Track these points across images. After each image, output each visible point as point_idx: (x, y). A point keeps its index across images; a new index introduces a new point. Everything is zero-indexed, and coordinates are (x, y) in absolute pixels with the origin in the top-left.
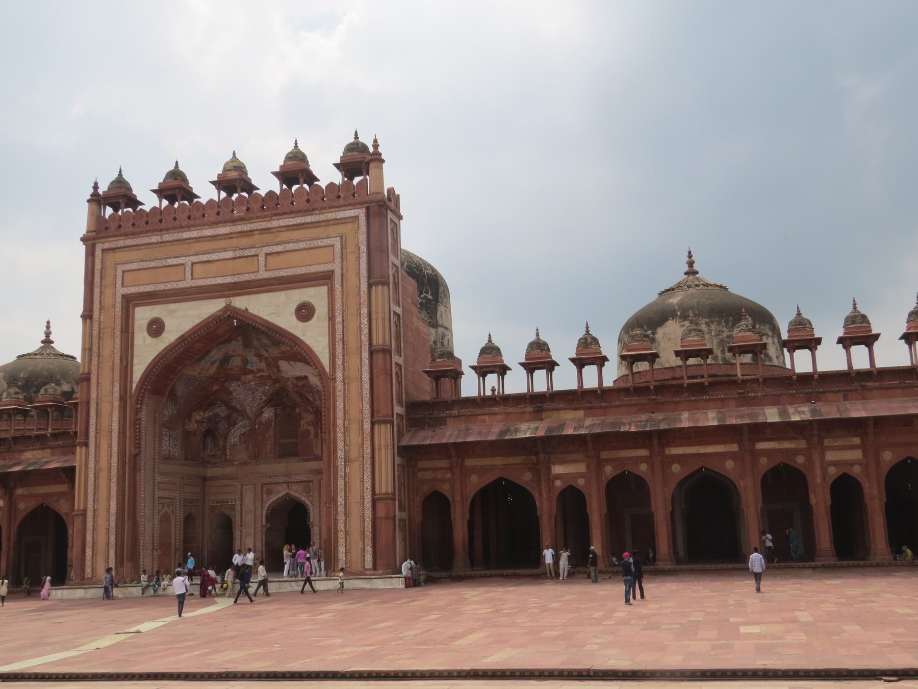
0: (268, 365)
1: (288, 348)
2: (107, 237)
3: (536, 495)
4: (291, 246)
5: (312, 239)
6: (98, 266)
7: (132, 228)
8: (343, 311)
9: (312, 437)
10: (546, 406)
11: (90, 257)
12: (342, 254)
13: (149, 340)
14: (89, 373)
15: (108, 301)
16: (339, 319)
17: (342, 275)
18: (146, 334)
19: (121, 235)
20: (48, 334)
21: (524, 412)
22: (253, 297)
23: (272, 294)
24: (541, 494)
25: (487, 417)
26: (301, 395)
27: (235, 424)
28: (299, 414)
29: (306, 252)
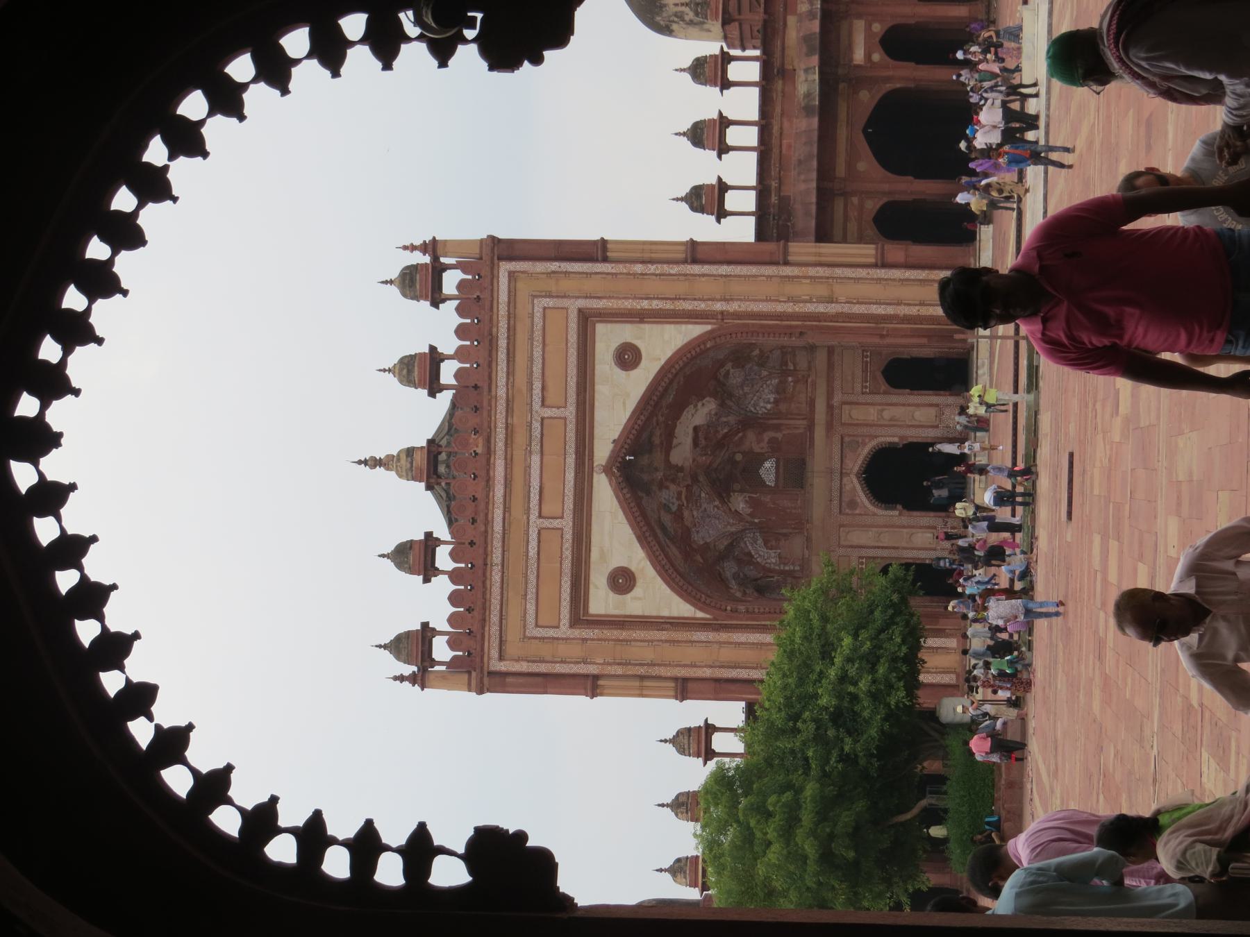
0: (673, 481)
1: (658, 433)
2: (482, 650)
3: (889, 86)
4: (537, 369)
5: (531, 339)
6: (524, 667)
7: (475, 613)
8: (635, 298)
9: (779, 435)
10: (777, 63)
11: (509, 680)
12: (557, 297)
13: (638, 591)
14: (675, 679)
15: (576, 651)
16: (645, 304)
17: (586, 297)
18: (629, 596)
21: (783, 92)
22: (598, 431)
23: (596, 404)
24: (888, 79)
25: (784, 142)
26: (720, 445)
27: (749, 554)
28: (744, 453)
29: (547, 349)
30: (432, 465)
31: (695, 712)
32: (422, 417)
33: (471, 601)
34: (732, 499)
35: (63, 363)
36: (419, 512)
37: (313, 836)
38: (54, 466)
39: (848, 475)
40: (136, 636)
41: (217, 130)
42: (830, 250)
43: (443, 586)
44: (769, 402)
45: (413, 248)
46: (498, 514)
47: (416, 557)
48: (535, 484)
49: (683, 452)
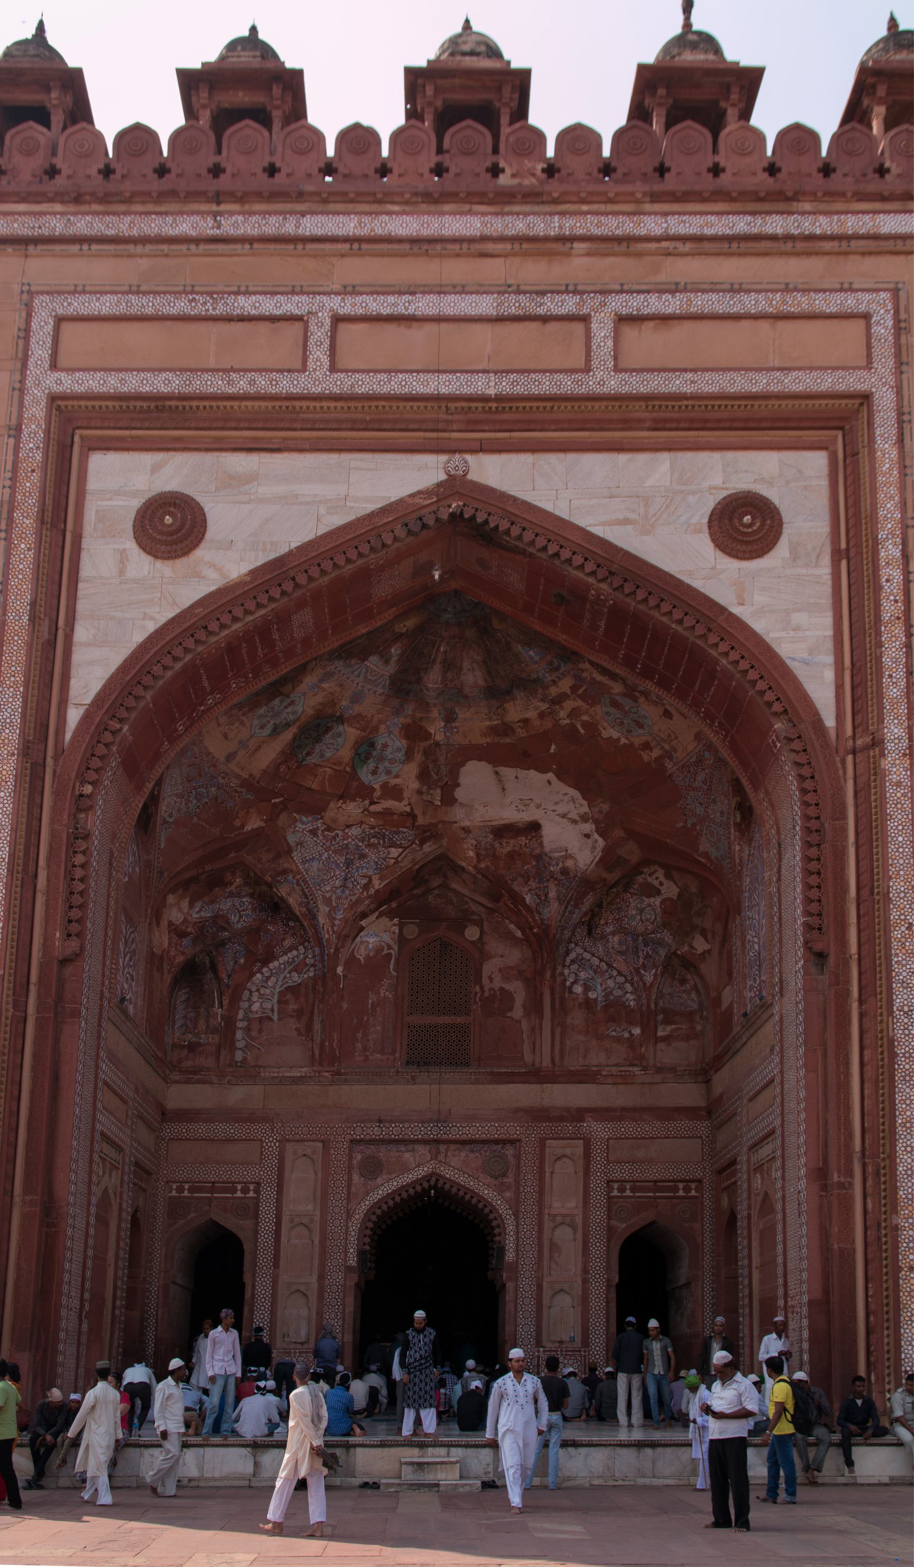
19: (59, 197)
30: (468, 96)
34: (385, 920)
39: (435, 1156)
44: (587, 988)
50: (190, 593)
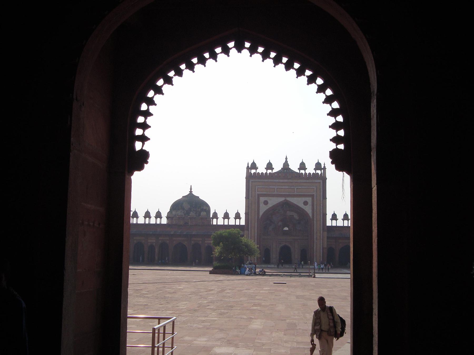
20: (191, 189)
31: (243, 216)
32: (294, 167)
33: (262, 176)
35: (258, 53)
36: (277, 167)
37: (147, 114)
38: (233, 52)
40: (194, 72)
41: (314, 87)
42: (325, 239)
43: (264, 171)
45: (324, 165)
46: (277, 181)
47: (269, 166)
48: (283, 187)
49: (289, 213)
50: (268, 208)
